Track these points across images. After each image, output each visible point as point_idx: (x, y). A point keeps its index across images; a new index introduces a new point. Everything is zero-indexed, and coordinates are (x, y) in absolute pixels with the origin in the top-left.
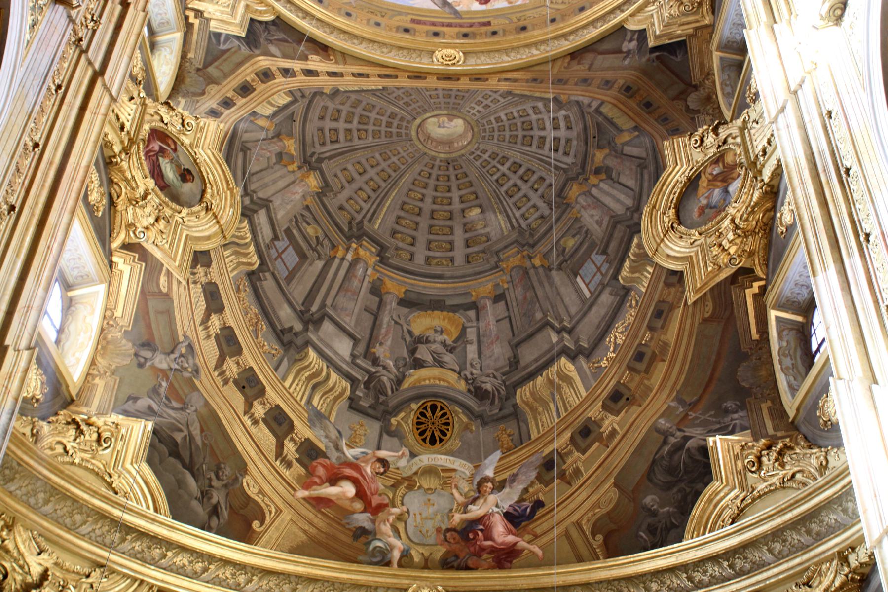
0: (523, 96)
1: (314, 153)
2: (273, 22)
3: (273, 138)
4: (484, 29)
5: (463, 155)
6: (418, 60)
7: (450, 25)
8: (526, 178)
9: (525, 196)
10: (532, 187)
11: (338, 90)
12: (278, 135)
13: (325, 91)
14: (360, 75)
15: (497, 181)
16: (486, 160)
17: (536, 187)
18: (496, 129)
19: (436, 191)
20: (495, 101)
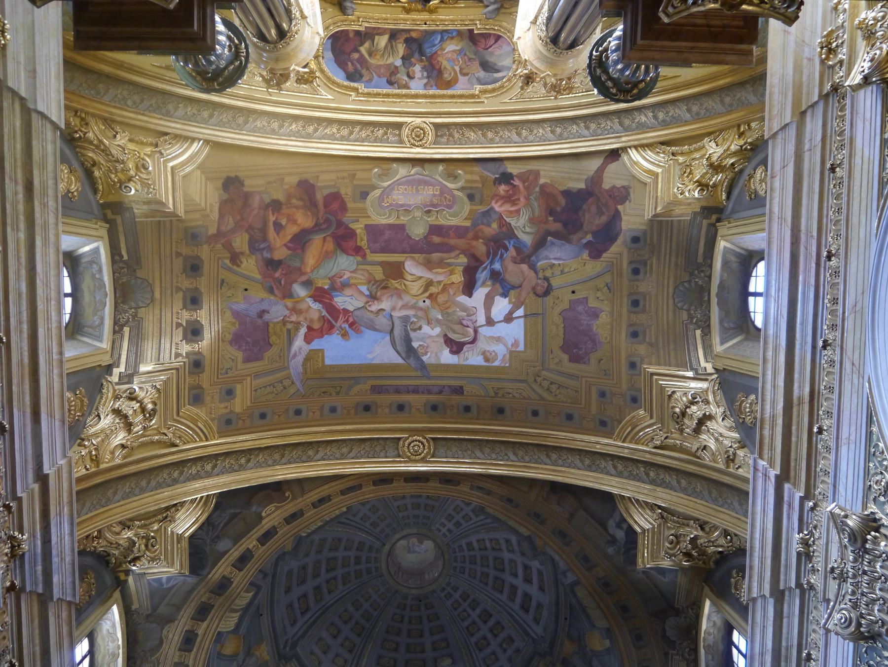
0: (496, 519)
1: (287, 641)
2: (217, 507)
3: (244, 661)
4: (456, 398)
5: (434, 591)
6: (382, 454)
7: (416, 390)
8: (495, 632)
9: (494, 653)
10: (501, 645)
11: (301, 538)
12: (249, 653)
13: (286, 550)
14: (322, 501)
15: (467, 628)
16: (457, 601)
17: (504, 646)
18: (467, 559)
19: (409, 636)
20: (467, 518)
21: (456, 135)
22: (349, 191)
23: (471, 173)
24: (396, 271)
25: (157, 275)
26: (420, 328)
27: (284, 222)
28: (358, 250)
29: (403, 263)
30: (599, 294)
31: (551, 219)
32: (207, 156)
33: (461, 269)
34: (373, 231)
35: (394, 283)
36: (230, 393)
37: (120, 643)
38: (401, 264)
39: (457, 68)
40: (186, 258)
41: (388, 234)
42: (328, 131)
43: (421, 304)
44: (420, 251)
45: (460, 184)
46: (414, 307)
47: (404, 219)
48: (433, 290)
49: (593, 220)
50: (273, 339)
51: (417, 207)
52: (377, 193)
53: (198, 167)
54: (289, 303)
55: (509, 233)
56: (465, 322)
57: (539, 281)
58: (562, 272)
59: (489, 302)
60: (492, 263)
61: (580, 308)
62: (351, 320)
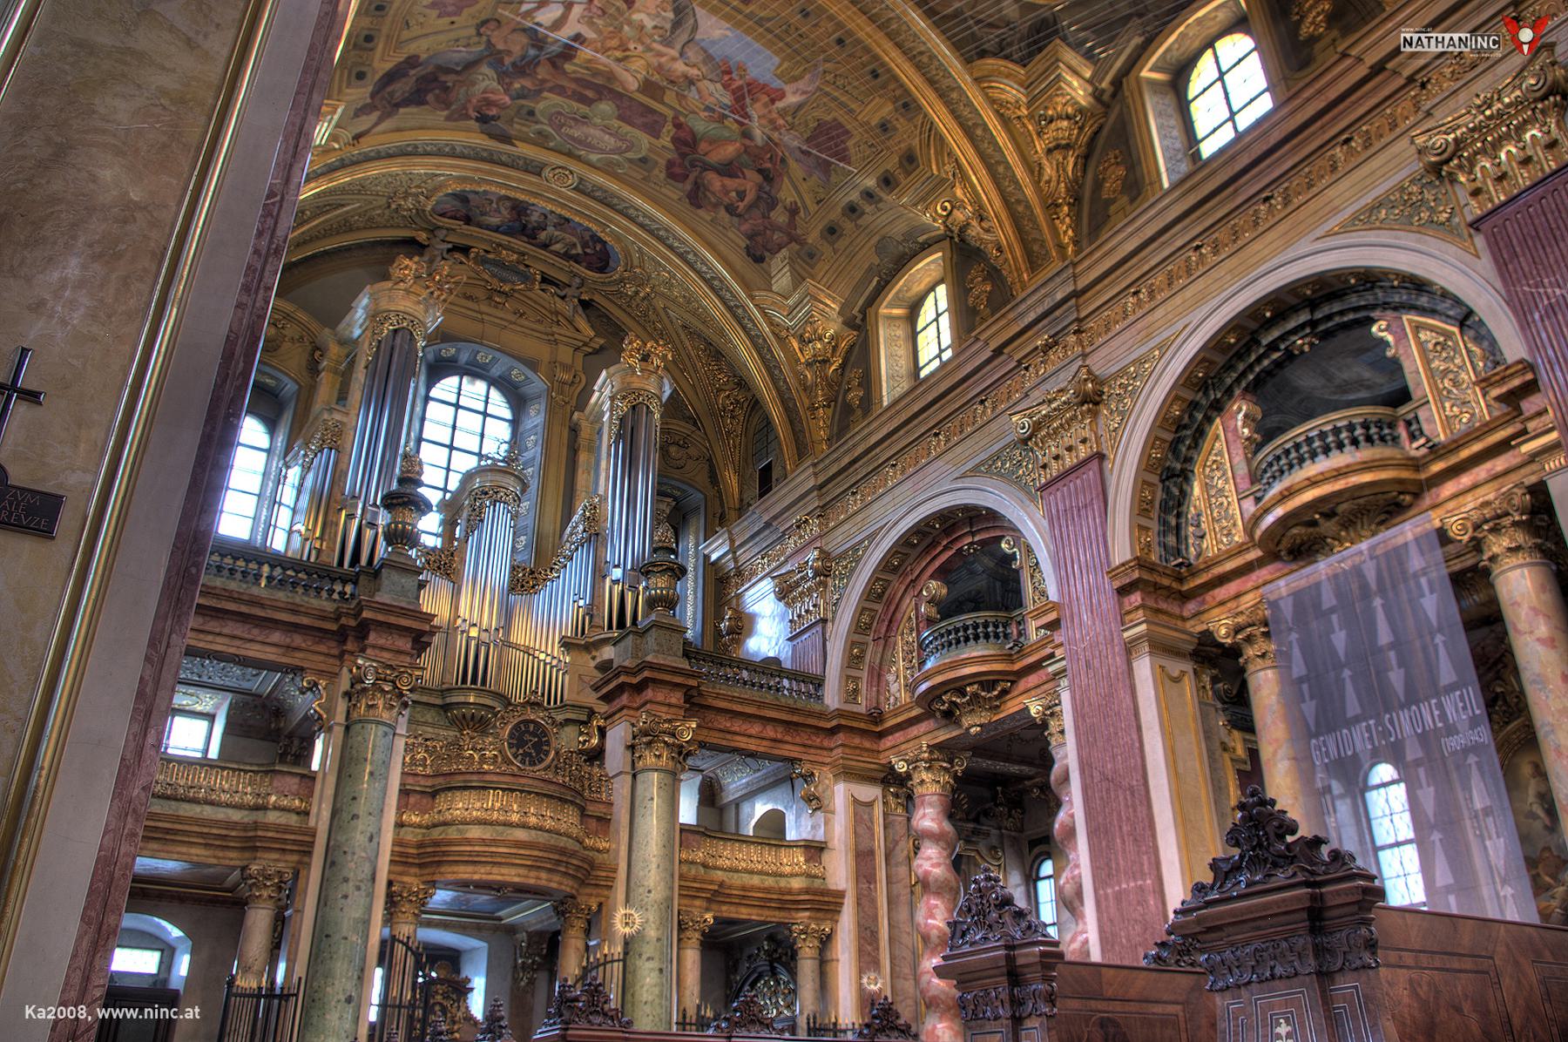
2: (983, 54)
21: (521, 163)
22: (656, 172)
23: (520, 131)
24: (648, 87)
25: (864, 250)
26: (655, 27)
27: (734, 194)
28: (678, 126)
29: (638, 90)
30: (422, 19)
31: (450, 84)
32: (759, 289)
33: (576, 61)
34: (654, 130)
35: (656, 78)
36: (884, 127)
37: (1182, 28)
38: (640, 90)
39: (494, 205)
40: (832, 244)
41: (639, 121)
42: (647, 222)
43: (640, 48)
44: (611, 91)
45: (538, 127)
46: (649, 49)
47: (616, 123)
48: (618, 54)
49: (401, 88)
50: (813, 125)
51: (595, 125)
52: (629, 155)
53: (771, 291)
54: (775, 135)
55: (502, 76)
56: (600, 12)
57: (489, 33)
58: (457, 40)
59: (558, 24)
60: (538, 56)
61: (450, 9)
62: (726, 78)
